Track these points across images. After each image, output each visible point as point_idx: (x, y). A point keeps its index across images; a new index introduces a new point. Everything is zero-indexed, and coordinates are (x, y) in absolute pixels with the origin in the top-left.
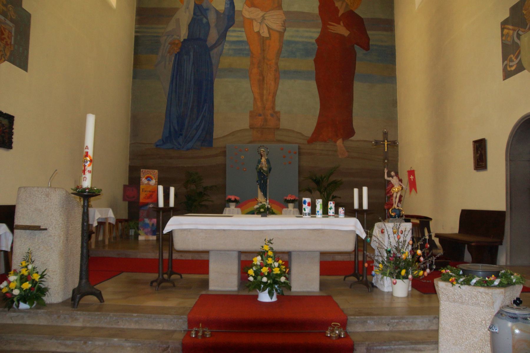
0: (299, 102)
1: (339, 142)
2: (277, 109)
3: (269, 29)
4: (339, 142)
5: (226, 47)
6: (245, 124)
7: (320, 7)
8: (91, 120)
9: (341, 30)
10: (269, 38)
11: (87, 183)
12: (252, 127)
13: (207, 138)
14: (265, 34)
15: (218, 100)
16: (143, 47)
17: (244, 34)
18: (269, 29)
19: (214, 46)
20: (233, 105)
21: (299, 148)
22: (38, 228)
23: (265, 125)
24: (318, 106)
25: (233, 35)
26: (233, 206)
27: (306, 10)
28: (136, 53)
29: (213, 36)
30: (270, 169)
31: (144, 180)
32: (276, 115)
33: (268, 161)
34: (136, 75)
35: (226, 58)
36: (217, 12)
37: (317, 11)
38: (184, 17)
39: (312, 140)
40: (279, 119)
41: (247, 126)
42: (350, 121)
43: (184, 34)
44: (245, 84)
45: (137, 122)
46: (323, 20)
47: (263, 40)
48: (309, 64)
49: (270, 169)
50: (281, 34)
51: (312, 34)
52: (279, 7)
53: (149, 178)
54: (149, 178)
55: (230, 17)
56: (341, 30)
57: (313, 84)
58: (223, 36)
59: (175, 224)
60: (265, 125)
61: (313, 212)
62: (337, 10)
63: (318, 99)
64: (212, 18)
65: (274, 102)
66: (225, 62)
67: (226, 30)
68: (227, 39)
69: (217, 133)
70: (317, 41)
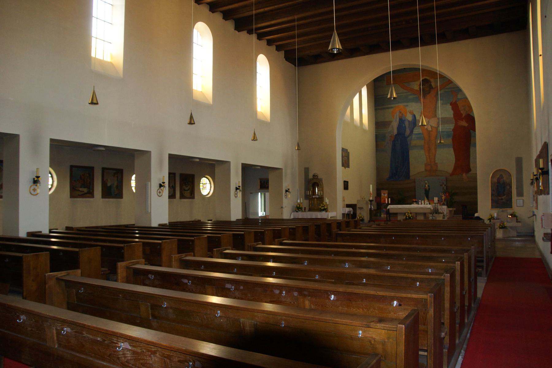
0: (446, 158)
1: (464, 175)
2: (436, 162)
3: (431, 127)
4: (464, 175)
5: (414, 136)
6: (423, 169)
7: (454, 115)
8: (371, 186)
9: (464, 124)
10: (432, 131)
11: (371, 199)
12: (426, 170)
13: (408, 176)
14: (430, 129)
15: (411, 160)
16: (379, 139)
17: (421, 130)
18: (431, 127)
19: (408, 137)
20: (417, 161)
21: (446, 178)
22: (362, 208)
23: (432, 169)
24: (454, 159)
25: (416, 131)
26: (415, 203)
27: (448, 116)
28: (376, 141)
29: (408, 132)
30: (429, 189)
31: (383, 195)
32: (436, 164)
33: (428, 186)
34: (376, 152)
35: (414, 141)
36: (409, 121)
37: (452, 116)
38: (395, 124)
39: (452, 174)
40: (437, 166)
41: (423, 169)
42: (469, 165)
43: (395, 132)
44: (422, 152)
45: (379, 170)
46: (455, 120)
47: (429, 132)
48: (450, 141)
49: (429, 189)
50: (437, 128)
51: (451, 127)
52: (436, 116)
53: (384, 194)
54: (384, 194)
55: (414, 122)
56: (464, 124)
57: (452, 150)
58: (412, 132)
59: (390, 207)
60: (432, 169)
61: (422, 204)
62: (462, 114)
63: (454, 156)
64: (407, 124)
65: (435, 159)
66: (414, 143)
67: (413, 129)
68: (414, 133)
69: (412, 173)
70: (454, 130)
